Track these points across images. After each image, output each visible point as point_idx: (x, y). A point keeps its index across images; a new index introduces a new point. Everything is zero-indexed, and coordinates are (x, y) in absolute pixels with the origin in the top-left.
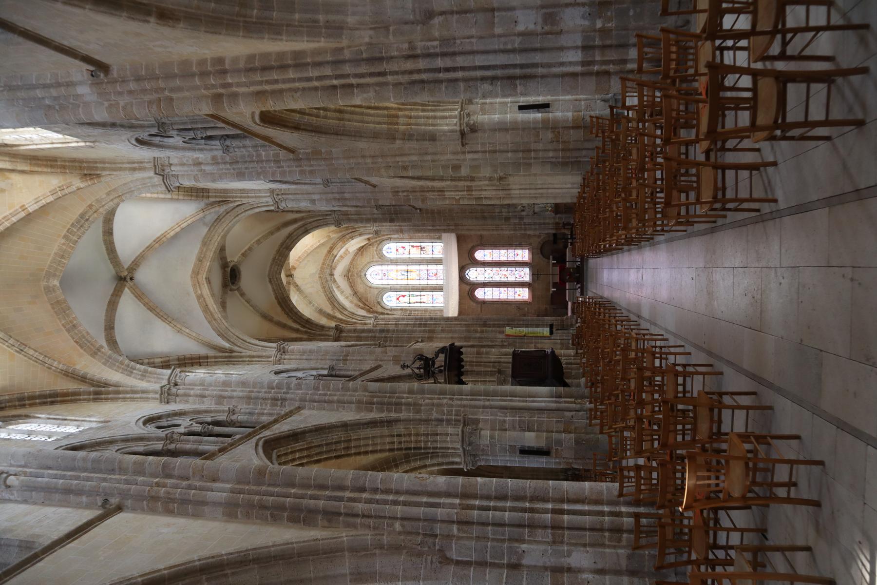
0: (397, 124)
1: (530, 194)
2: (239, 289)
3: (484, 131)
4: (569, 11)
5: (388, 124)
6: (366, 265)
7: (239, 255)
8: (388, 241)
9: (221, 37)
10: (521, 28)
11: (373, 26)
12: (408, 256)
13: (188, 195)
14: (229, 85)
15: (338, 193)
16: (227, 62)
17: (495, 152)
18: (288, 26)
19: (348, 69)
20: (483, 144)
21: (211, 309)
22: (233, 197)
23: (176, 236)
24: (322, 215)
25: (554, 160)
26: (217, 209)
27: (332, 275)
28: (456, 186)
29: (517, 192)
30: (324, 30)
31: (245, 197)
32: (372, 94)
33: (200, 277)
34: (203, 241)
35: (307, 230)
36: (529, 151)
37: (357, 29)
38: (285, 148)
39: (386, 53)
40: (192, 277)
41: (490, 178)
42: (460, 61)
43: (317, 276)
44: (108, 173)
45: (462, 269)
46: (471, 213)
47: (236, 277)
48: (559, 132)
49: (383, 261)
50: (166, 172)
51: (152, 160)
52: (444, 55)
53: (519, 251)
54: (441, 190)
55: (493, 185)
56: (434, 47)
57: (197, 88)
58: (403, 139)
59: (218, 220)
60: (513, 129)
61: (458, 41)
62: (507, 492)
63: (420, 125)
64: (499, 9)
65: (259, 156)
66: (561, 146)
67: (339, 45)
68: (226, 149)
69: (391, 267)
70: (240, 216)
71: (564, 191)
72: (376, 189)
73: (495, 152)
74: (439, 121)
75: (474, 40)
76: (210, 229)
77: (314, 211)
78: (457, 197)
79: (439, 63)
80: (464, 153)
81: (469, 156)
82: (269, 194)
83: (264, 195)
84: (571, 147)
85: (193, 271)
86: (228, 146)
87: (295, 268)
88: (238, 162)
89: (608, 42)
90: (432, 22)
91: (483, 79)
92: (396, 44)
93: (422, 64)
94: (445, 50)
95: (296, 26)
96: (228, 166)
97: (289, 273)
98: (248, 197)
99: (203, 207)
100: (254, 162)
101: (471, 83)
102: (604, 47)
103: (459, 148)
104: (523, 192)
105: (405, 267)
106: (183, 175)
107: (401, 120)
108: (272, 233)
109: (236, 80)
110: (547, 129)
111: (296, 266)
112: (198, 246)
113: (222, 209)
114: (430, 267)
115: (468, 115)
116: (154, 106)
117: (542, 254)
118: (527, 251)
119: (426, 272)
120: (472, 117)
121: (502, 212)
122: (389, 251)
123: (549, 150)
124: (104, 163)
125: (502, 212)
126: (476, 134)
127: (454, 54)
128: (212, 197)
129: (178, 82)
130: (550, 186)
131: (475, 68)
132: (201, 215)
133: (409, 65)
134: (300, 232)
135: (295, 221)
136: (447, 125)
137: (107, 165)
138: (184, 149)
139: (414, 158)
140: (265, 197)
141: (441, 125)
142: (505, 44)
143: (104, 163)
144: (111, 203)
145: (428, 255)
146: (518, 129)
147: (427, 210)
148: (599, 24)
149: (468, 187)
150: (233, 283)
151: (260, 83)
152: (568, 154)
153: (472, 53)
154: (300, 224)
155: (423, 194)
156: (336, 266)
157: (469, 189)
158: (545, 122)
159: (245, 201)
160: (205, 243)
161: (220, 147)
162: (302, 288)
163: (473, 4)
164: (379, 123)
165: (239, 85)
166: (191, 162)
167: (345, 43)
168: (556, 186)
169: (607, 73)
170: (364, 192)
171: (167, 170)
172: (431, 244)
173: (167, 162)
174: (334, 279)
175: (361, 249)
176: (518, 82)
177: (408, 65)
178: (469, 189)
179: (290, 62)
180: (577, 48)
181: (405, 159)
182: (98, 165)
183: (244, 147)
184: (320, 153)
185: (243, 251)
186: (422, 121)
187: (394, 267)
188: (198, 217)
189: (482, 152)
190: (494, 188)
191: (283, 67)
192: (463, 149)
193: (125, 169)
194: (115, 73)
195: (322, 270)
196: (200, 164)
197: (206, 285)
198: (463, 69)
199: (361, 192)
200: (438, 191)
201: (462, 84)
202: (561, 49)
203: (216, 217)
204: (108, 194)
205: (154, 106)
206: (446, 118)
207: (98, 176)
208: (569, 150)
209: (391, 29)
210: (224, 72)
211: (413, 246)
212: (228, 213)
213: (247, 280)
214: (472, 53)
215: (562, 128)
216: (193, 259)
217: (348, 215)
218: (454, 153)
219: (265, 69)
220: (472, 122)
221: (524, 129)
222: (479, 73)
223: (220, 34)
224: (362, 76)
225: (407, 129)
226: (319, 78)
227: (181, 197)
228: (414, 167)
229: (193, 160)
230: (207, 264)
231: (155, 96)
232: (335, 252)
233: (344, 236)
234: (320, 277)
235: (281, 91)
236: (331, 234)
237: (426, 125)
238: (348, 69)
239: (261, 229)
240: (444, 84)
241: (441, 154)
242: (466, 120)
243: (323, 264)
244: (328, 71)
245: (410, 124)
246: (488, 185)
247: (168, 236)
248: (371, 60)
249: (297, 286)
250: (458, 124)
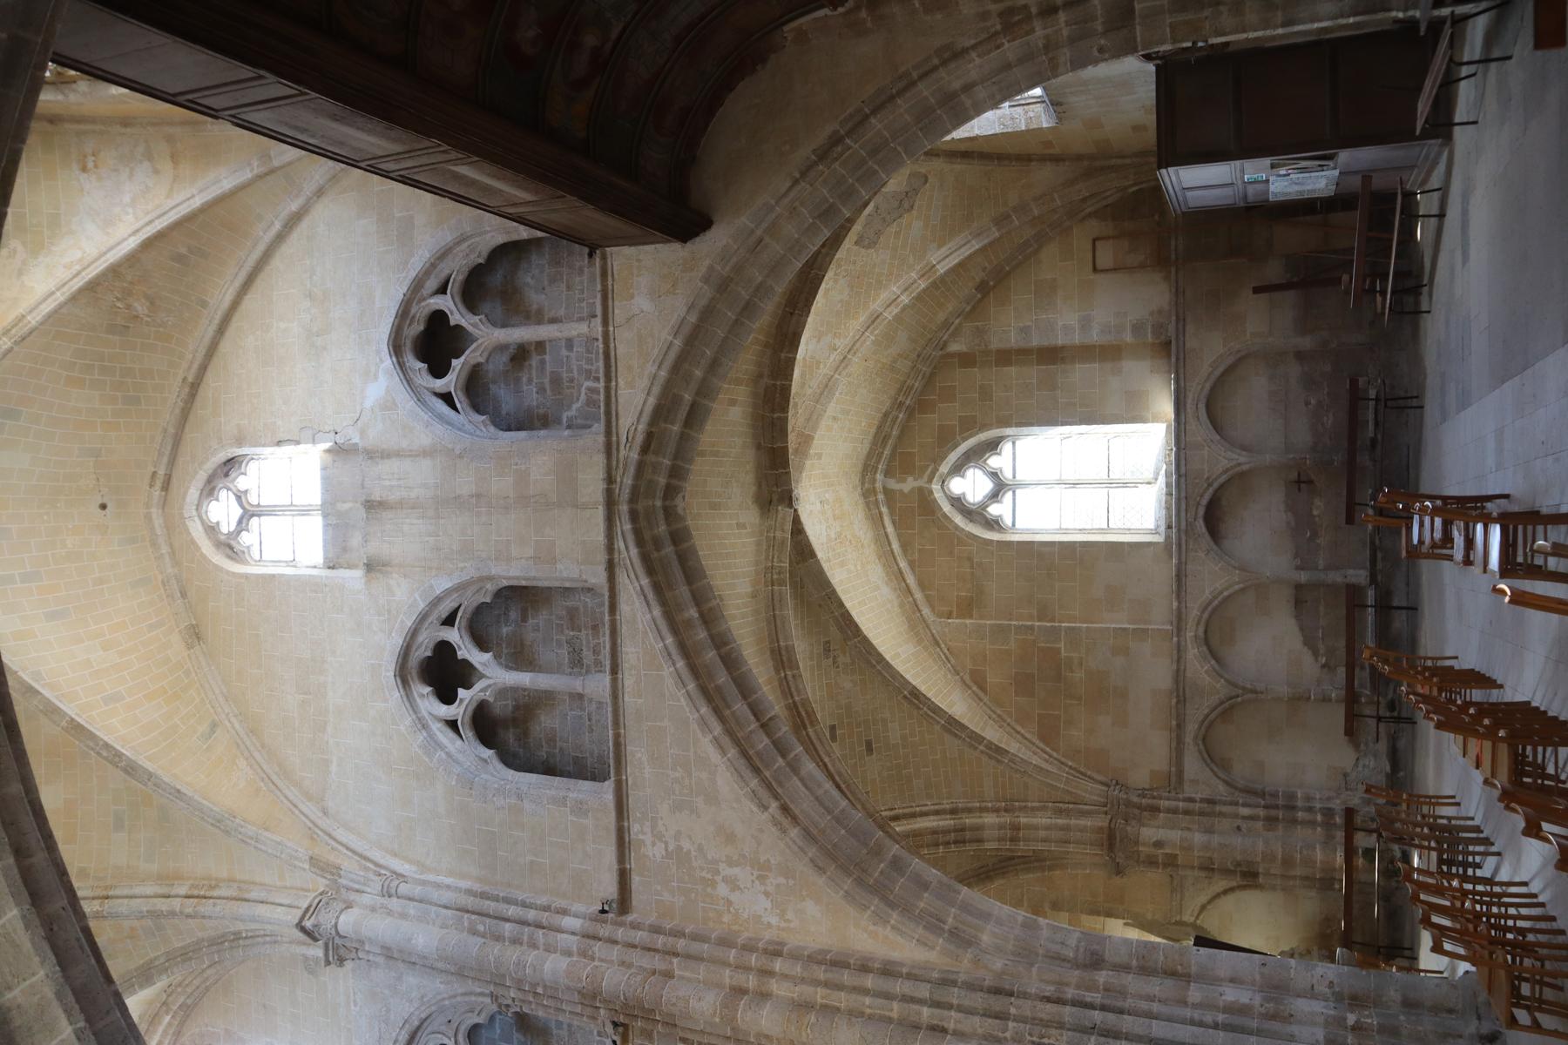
9: (821, 881)
52: (1103, 1008)
79: (1097, 1016)
92: (1035, 981)
151: (816, 983)
153: (1150, 1015)
163: (1162, 958)
191: (864, 968)
194: (629, 918)
210: (777, 954)
214: (1150, 1015)
224: (970, 1012)
238: (955, 996)
244: (923, 991)
248: (997, 991)
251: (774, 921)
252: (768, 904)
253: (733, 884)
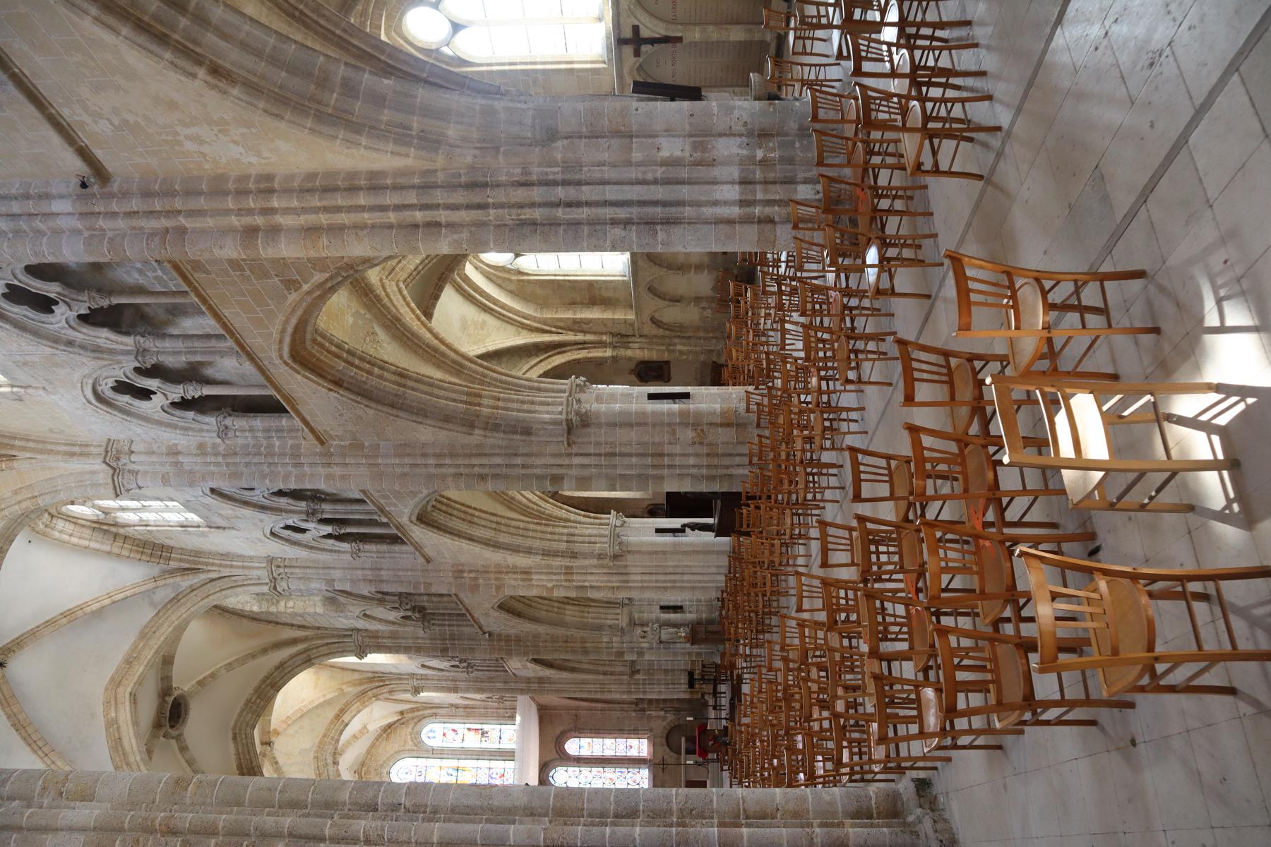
0: (479, 405)
1: (657, 581)
2: (178, 738)
3: (599, 425)
4: (722, 140)
5: (465, 403)
6: (392, 755)
7: (194, 682)
8: (432, 719)
9: (282, 125)
10: (665, 154)
11: (479, 145)
12: (461, 745)
13: (137, 552)
14: (272, 211)
15: (371, 569)
16: (277, 180)
17: (614, 455)
18: (371, 127)
19: (439, 196)
20: (598, 444)
21: (126, 745)
22: (207, 564)
23: (99, 614)
24: (338, 636)
25: (695, 471)
26: (178, 579)
27: (336, 763)
28: (550, 566)
29: (639, 578)
30: (416, 141)
31: (226, 566)
32: (465, 235)
33: (120, 690)
34: (141, 632)
35: (310, 660)
36: (661, 455)
37: (458, 147)
38: (312, 430)
39: (491, 177)
40: (106, 689)
41: (600, 555)
42: (587, 193)
43: (312, 755)
44: (28, 455)
45: (544, 768)
46: (566, 642)
47: (179, 717)
48: (702, 431)
49: (421, 750)
50: (120, 463)
51: (104, 444)
52: (565, 183)
53: (634, 742)
54: (527, 572)
55: (603, 567)
56: (554, 173)
57: (227, 212)
58: (486, 429)
59: (176, 600)
60: (639, 424)
61: (585, 169)
62: (637, 804)
63: (512, 410)
64: (638, 136)
65: (270, 446)
66: (705, 450)
67: (431, 166)
68: (223, 432)
69: (431, 762)
70: (211, 597)
71: (706, 578)
72: (430, 566)
73: (614, 455)
74: (537, 408)
75: (605, 168)
76: (157, 614)
77: (326, 629)
78: (550, 585)
79: (560, 193)
80: (569, 455)
81: (577, 461)
82: (264, 565)
83: (257, 565)
84: (720, 451)
85: (112, 679)
86: (226, 428)
87: (277, 733)
88: (235, 454)
89: (771, 176)
90: (554, 145)
91: (614, 222)
93: (537, 194)
94: (568, 177)
95: (382, 130)
96: (220, 459)
97: (266, 739)
98: (232, 566)
99: (156, 575)
100: (260, 455)
101: (598, 227)
102: (766, 182)
104: (646, 577)
105: (454, 763)
106: (146, 472)
107: (485, 401)
108: (253, 656)
109: (284, 204)
110: (687, 425)
111: (280, 730)
112: (132, 638)
113: (186, 582)
114: (493, 764)
116: (157, 240)
117: (668, 745)
118: (645, 742)
119: (487, 771)
121: (611, 642)
122: (431, 735)
123: (688, 455)
124: (28, 440)
125: (611, 642)
126: (588, 430)
127: (579, 183)
128: (175, 560)
129: (202, 203)
130: (687, 570)
131: (606, 203)
132: (151, 586)
133: (520, 195)
134: (298, 660)
135: (294, 641)
136: (548, 413)
137: (31, 444)
138: (159, 423)
139: (498, 460)
140: (259, 568)
141: (540, 412)
142: (645, 173)
143: (28, 440)
144: (17, 507)
145: (492, 744)
146: (645, 424)
147: (500, 635)
148: (760, 154)
149: (567, 567)
150: (172, 727)
151: (316, 210)
152: (715, 461)
153: (604, 183)
154: (300, 647)
155: (500, 576)
156: (343, 751)
157: (568, 571)
159: (225, 572)
160: (144, 635)
161: (216, 428)
162: (283, 769)
163: (607, 123)
164: (454, 400)
165: (286, 211)
166: (164, 449)
167: (440, 161)
168: (694, 570)
169: (771, 221)
170: (412, 570)
171: (124, 460)
172: (498, 727)
173: (126, 448)
174: (338, 770)
175: (388, 729)
176: (659, 227)
177: (519, 192)
178: (568, 571)
179: (363, 182)
180: (732, 183)
181: (484, 461)
182: (17, 443)
183: (252, 430)
184: (362, 446)
185: (201, 677)
186: (515, 405)
187: (436, 762)
188: (143, 588)
189: (596, 455)
190: (605, 571)
191: (353, 189)
192: (569, 451)
193: (58, 453)
194: (115, 187)
195: (321, 746)
196: (178, 453)
197: (127, 703)
198: (588, 204)
199: (407, 570)
200: (523, 573)
201: (586, 229)
202: (714, 182)
203: (173, 595)
204: (16, 493)
205: (157, 240)
206: (548, 404)
207: (12, 458)
208: (717, 455)
209: (502, 149)
210: (271, 191)
211: (469, 729)
212: (192, 591)
213: (196, 725)
214: (604, 183)
215: (707, 424)
216: (119, 658)
217: (377, 637)
218: (555, 455)
219: (327, 190)
220: (584, 411)
221: (654, 425)
222: (609, 212)
223: (282, 118)
224: (455, 207)
225: (493, 413)
226: (399, 208)
227: (125, 553)
228: (496, 476)
229: (168, 447)
230: (139, 669)
231: (165, 223)
232: (346, 718)
233: (364, 693)
234: (316, 758)
235: (342, 228)
236: (344, 687)
237: (519, 411)
238: (439, 196)
239: (235, 648)
240: (561, 230)
241: (537, 455)
242: (575, 407)
243: (325, 736)
244: (411, 198)
246: (595, 567)
247: (88, 610)
248: (472, 186)
249: (277, 763)
250: (564, 411)
251: (254, 160)
252: (241, 149)
253: (197, 139)
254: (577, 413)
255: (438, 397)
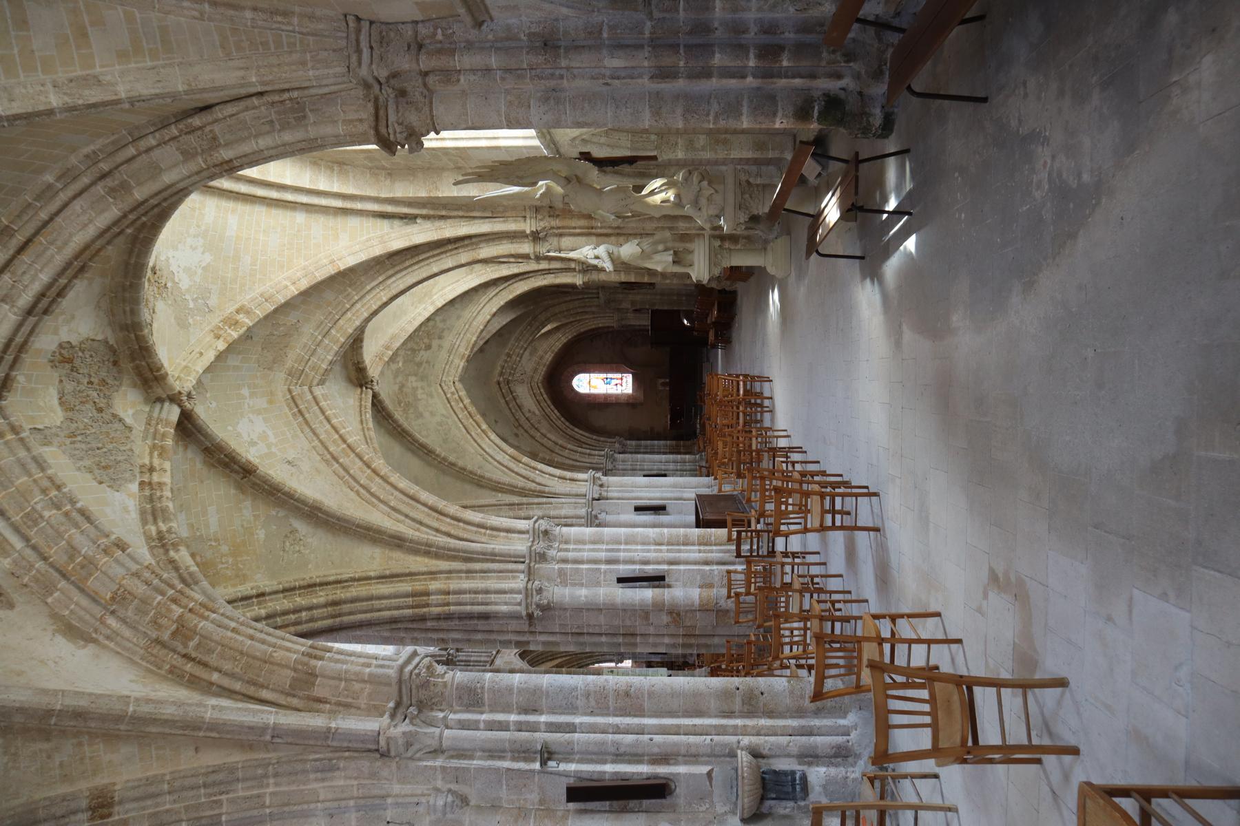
0: (427, 605)
5: (412, 607)
66: (681, 631)
103: (526, 628)
115: (540, 591)
120: (545, 594)
136: (506, 604)
141: (496, 604)
158: (658, 607)
206: (504, 592)
220: (546, 602)
242: (536, 598)
245: (448, 604)
250: (524, 604)
254: (538, 606)
255: (379, 610)
